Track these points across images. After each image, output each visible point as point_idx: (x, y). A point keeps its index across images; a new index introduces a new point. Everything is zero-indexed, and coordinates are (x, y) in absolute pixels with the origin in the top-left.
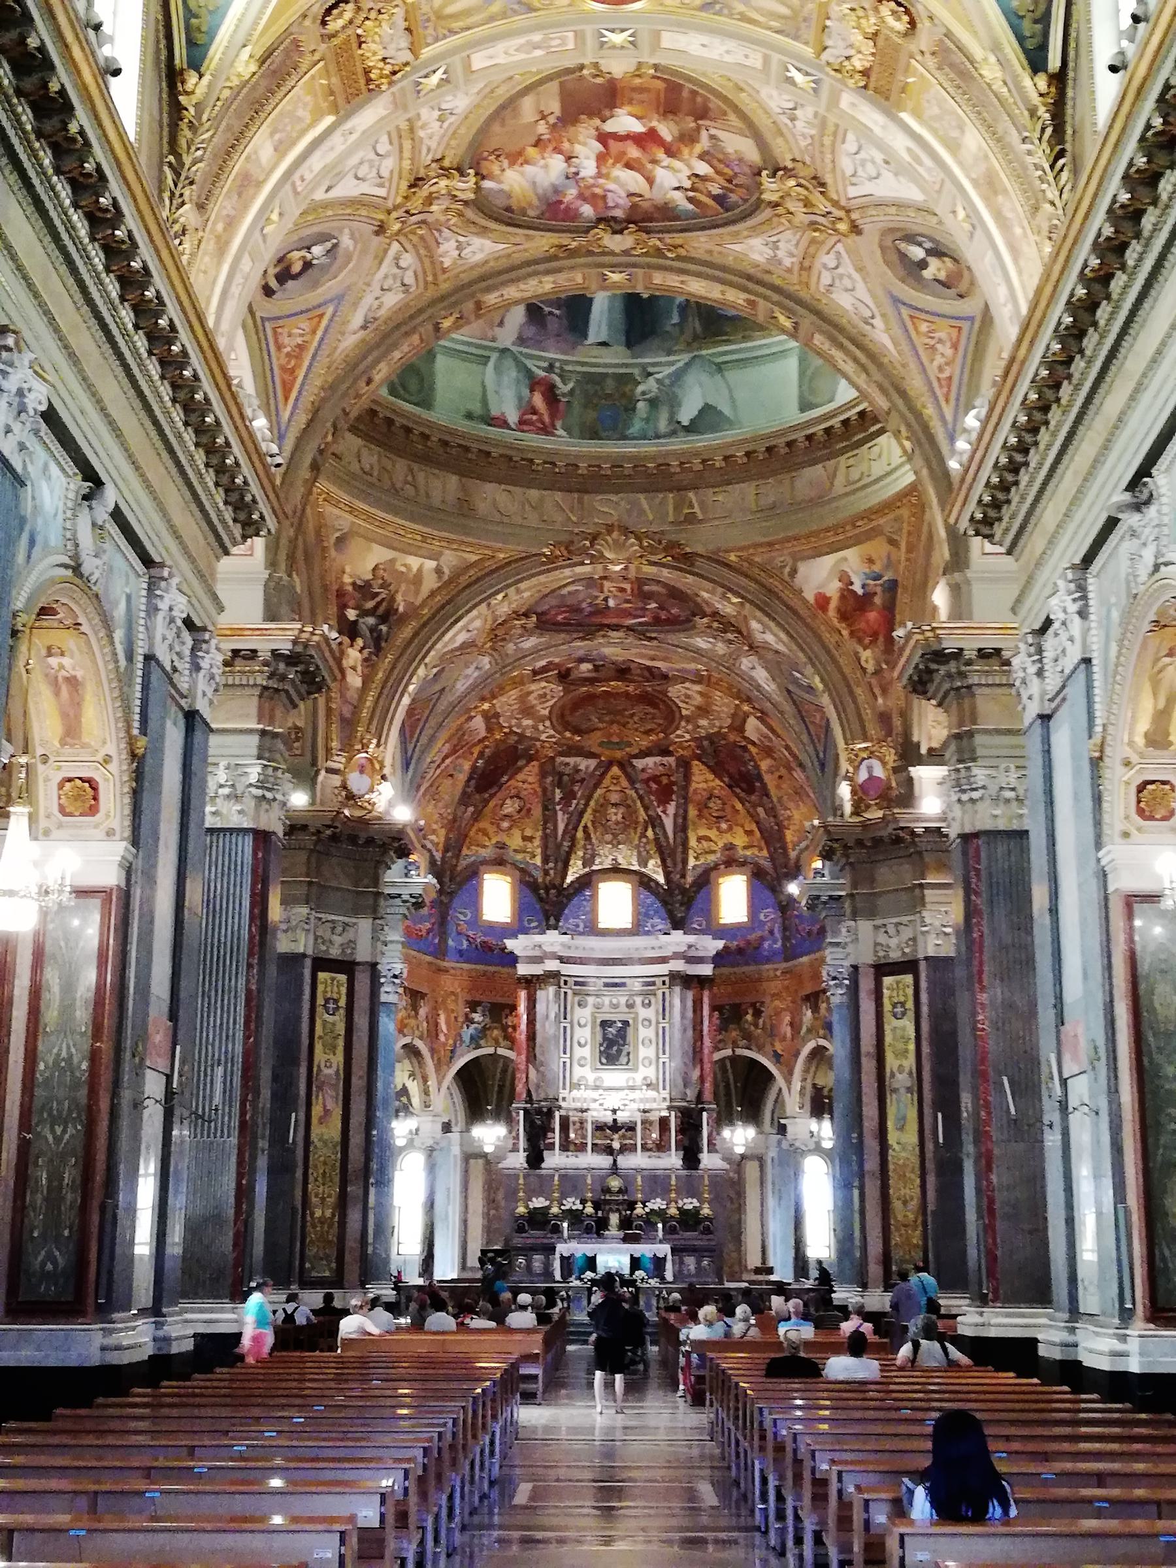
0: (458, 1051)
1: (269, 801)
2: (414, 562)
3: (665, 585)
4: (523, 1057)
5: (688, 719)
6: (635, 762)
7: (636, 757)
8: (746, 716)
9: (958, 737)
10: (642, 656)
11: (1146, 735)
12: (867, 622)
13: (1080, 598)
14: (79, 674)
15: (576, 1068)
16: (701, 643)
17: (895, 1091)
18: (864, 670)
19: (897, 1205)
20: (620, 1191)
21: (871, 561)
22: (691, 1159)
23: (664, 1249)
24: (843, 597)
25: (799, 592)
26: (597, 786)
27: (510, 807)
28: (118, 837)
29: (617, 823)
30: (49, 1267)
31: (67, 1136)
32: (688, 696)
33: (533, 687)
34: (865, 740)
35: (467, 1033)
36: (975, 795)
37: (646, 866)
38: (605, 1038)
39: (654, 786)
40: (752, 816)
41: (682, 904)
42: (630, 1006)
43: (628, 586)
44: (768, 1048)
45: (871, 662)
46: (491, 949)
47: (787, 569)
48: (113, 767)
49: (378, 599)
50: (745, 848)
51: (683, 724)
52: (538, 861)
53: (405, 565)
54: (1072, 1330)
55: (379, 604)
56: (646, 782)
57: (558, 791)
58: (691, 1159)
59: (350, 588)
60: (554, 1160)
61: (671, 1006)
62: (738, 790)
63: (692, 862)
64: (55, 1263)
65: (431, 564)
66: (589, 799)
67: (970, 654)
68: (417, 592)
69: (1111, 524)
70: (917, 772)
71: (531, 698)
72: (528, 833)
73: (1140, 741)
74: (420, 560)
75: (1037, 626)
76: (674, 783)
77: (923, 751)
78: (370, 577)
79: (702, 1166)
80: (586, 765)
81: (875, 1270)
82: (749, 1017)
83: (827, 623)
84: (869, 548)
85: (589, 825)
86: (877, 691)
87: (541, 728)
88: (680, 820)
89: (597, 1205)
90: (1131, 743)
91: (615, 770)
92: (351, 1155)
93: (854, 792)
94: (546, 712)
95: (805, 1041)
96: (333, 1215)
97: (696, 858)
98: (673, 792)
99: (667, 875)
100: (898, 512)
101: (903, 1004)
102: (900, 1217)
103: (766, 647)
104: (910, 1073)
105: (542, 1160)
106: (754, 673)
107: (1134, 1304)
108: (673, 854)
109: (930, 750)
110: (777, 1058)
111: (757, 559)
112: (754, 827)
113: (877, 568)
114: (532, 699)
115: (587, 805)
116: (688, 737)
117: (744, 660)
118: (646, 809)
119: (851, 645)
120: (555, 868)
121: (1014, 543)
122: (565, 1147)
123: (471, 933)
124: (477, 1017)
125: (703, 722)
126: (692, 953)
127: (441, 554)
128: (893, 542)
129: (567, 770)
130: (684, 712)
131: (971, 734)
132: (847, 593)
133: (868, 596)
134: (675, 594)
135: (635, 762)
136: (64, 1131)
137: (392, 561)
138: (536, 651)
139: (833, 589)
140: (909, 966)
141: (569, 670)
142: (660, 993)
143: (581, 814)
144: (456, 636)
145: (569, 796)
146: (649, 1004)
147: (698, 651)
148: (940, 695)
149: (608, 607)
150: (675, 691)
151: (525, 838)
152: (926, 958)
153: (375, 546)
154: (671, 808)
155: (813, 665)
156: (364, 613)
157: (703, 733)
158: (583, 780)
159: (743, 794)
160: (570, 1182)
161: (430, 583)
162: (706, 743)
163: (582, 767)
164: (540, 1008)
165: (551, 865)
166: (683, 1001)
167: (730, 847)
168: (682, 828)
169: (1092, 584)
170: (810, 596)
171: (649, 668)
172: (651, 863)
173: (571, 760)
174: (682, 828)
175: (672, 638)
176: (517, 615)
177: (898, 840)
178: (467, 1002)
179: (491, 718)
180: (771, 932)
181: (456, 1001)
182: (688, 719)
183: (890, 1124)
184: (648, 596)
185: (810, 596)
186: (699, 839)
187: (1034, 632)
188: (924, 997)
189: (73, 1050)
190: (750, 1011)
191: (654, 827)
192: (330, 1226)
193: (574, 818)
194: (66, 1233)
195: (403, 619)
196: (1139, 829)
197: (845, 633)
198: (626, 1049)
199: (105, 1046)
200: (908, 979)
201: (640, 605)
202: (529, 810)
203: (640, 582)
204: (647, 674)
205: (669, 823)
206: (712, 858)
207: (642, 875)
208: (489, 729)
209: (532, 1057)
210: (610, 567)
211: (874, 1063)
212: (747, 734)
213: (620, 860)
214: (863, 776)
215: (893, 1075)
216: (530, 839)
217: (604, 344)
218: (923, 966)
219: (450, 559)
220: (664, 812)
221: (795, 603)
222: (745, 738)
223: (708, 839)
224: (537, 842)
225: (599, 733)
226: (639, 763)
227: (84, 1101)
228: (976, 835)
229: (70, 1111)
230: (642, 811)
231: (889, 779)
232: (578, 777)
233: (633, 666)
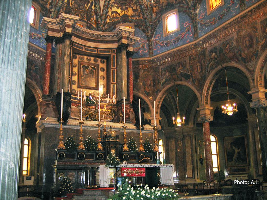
37: (89, 21)
50: (131, 16)
63: (108, 21)
97: (110, 20)
108: (102, 15)
112: (138, 7)
165: (53, 10)
172: (92, 19)
180: (143, 47)
191: (95, 5)
223: (116, 12)
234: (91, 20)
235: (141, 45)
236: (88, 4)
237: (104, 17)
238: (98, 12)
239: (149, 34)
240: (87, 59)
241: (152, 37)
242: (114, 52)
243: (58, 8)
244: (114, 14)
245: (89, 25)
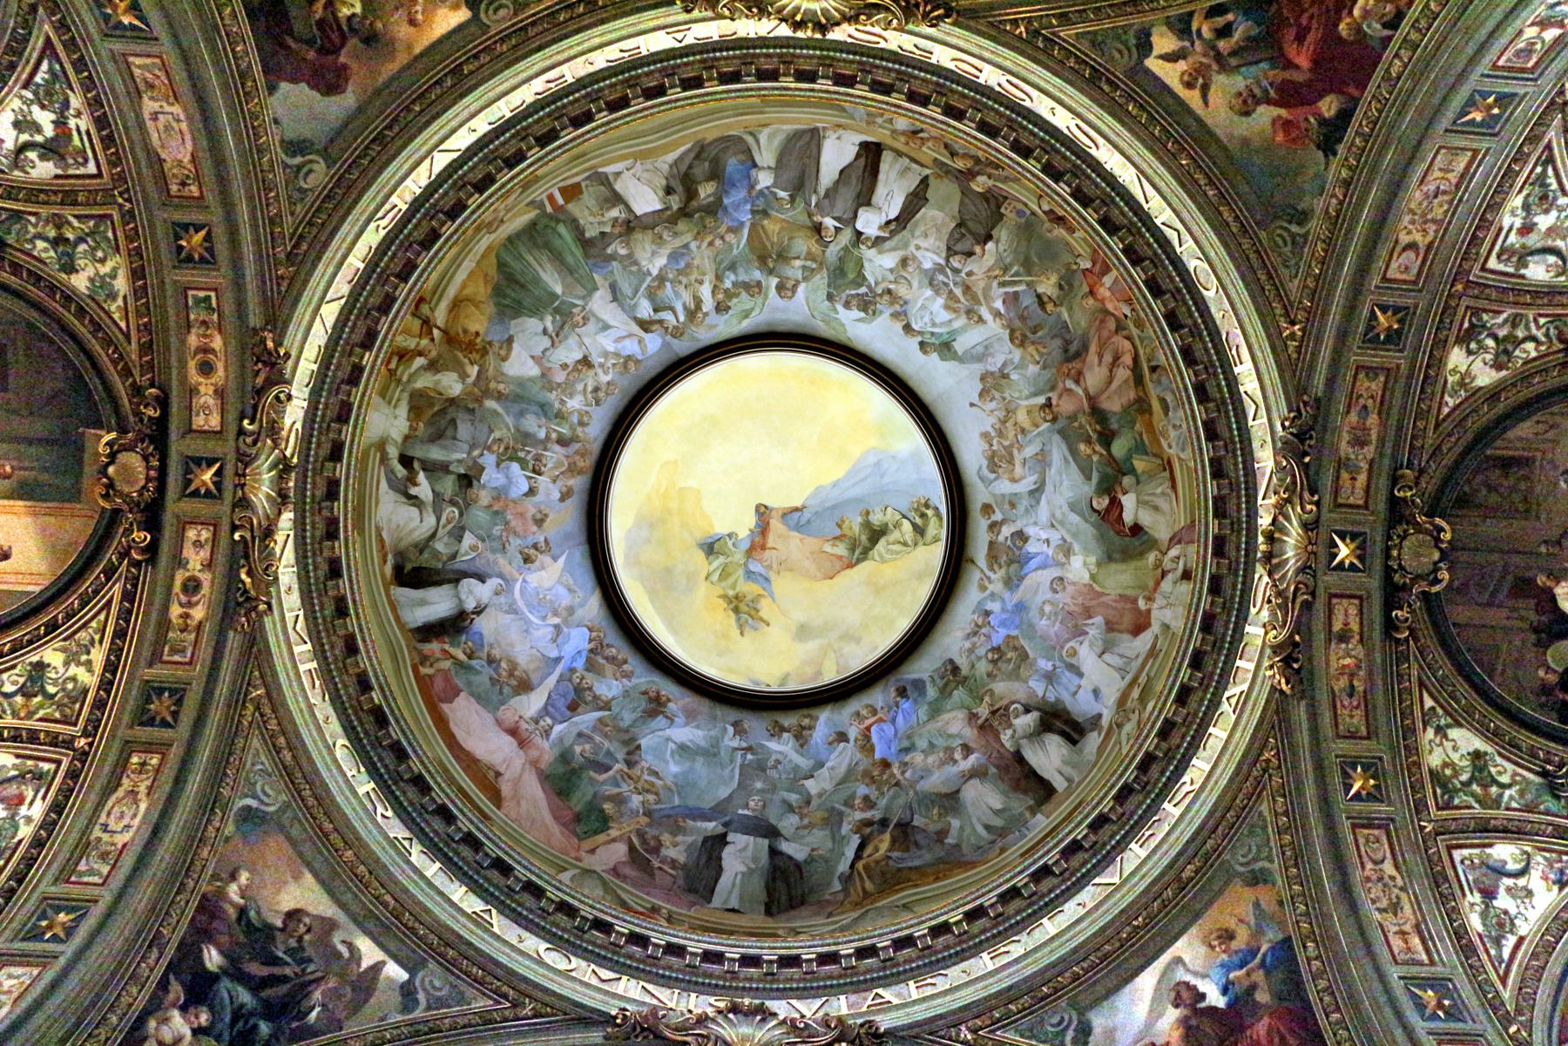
2: (369, 952)
53: (350, 946)
59: (232, 913)
65: (395, 972)
68: (356, 1007)
74: (378, 955)
78: (279, 923)
113: (1241, 941)
128: (1257, 879)
133: (1241, 1005)
137: (330, 925)
153: (309, 878)
161: (384, 1003)
217: (733, 910)
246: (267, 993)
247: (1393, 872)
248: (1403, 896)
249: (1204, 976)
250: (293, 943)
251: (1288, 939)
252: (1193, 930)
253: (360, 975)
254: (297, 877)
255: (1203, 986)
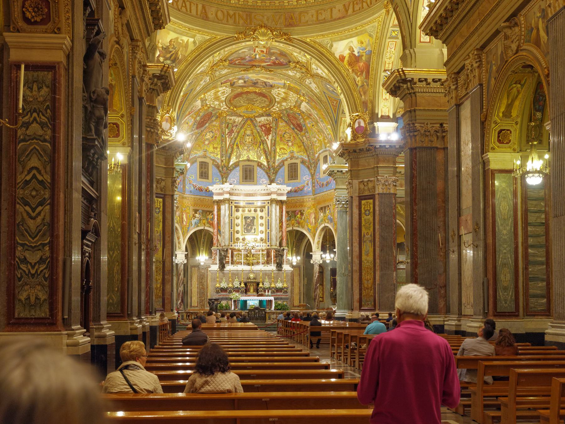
0: (191, 228)
1: (152, 133)
2: (185, 39)
3: (279, 50)
4: (216, 230)
5: (278, 103)
6: (256, 119)
7: (257, 117)
8: (302, 101)
9: (410, 111)
10: (262, 77)
11: (503, 113)
12: (359, 67)
13: (479, 61)
14: (113, 83)
15: (236, 234)
16: (290, 73)
17: (365, 242)
18: (357, 85)
19: (365, 282)
20: (254, 278)
21: (362, 43)
22: (279, 265)
23: (272, 298)
24: (350, 57)
25: (333, 54)
26: (241, 128)
27: (209, 136)
28: (127, 145)
29: (249, 142)
30: (111, 301)
31: (114, 255)
32: (279, 94)
33: (220, 89)
34: (358, 112)
35: (193, 221)
36: (416, 133)
38: (246, 223)
39: (264, 128)
40: (301, 141)
41: (273, 173)
42: (255, 211)
43: (265, 50)
44: (306, 226)
45: (360, 82)
46: (202, 190)
47: (329, 45)
48: (125, 119)
49: (172, 53)
51: (276, 104)
52: (219, 156)
53: (182, 40)
54: (459, 321)
55: (172, 55)
56: (261, 127)
57: (227, 130)
58: (279, 265)
60: (229, 268)
61: (271, 211)
62: (296, 130)
63: (277, 157)
64: (113, 300)
65: (191, 40)
66: (239, 133)
67: (416, 80)
68: (186, 51)
69: (497, 32)
70: (378, 125)
71: (219, 93)
72: (215, 146)
73: (501, 115)
75: (456, 71)
76: (272, 127)
77: (379, 116)
79: (283, 269)
80: (238, 120)
81: (356, 304)
82: (299, 216)
83: (343, 67)
84: (361, 37)
85: (239, 143)
86: (362, 93)
87: (222, 105)
88: (273, 142)
89: (245, 284)
90: (498, 116)
91: (249, 122)
92: (166, 265)
93: (353, 132)
94: (224, 99)
95: (321, 224)
96: (160, 287)
98: (271, 131)
99: (268, 162)
100: (374, 24)
101: (369, 210)
102: (366, 286)
103: (318, 75)
104: (371, 235)
105: (225, 268)
106: (310, 86)
107: (488, 310)
108: (270, 153)
109: (382, 116)
110: (309, 230)
111: (317, 41)
114: (219, 94)
115: (237, 136)
116: (277, 109)
117: (307, 80)
118: (260, 137)
119: (354, 75)
120: (225, 159)
121: (446, 40)
122: (232, 263)
123: (194, 184)
124: (197, 215)
125: (284, 104)
126: (279, 192)
127: (195, 36)
129: (231, 122)
130: (277, 100)
131: (415, 111)
132: (352, 55)
134: (283, 54)
135: (256, 119)
136: (113, 253)
137: (177, 38)
138: (226, 75)
139: (346, 53)
140: (372, 197)
141: (234, 82)
142: (266, 207)
143: (236, 139)
144: (200, 69)
145: (231, 132)
146: (263, 211)
147: (289, 76)
148: (403, 95)
149: (256, 58)
150: (274, 92)
151: (214, 148)
152: (378, 194)
153: (171, 32)
154: (270, 137)
155: (338, 83)
156: (166, 59)
157: (283, 108)
158: (237, 126)
159: (298, 132)
160: (235, 274)
161: (191, 47)
162: (285, 112)
163: (237, 121)
164: (222, 212)
165: (224, 158)
166: (276, 210)
167: (292, 152)
168: (274, 144)
169: (484, 57)
170: (337, 56)
171: (265, 83)
172: (262, 157)
173: (233, 118)
174: (274, 144)
175: (279, 71)
176: (221, 60)
177: (368, 150)
178: (193, 210)
179: (203, 100)
180: (308, 184)
181: (189, 209)
182: (278, 103)
183: (363, 254)
184: (273, 54)
185: (337, 56)
186: (280, 149)
187: (455, 73)
188: (377, 208)
189: (115, 224)
190: (299, 214)
191: (263, 144)
192: (160, 291)
193: (233, 141)
194: (116, 289)
195: (180, 62)
196: (498, 147)
197: (350, 70)
198: (254, 228)
199: (126, 223)
200: (371, 201)
201: (269, 57)
202: (216, 137)
203: (269, 49)
204: (264, 84)
205: (269, 143)
206: (285, 156)
207: (259, 162)
208: (202, 106)
209: (219, 231)
210: (260, 42)
211: (358, 232)
212: (301, 109)
213: (250, 156)
214: (356, 125)
215: (364, 236)
216: (216, 148)
218: (377, 196)
219: (199, 37)
220: (267, 138)
221: (331, 58)
222: (300, 110)
223: (284, 149)
224: (218, 150)
225: (243, 108)
226: (258, 119)
227: (120, 243)
228: (415, 149)
229: (115, 246)
230: (258, 137)
231: (366, 127)
232: (235, 124)
233: (259, 81)
234: (261, 159)
235: (306, 182)
236: (256, 145)
237: (272, 155)
238: (267, 150)
239: (313, 171)
240: (248, 210)
241: (314, 174)
242: (268, 203)
243: (229, 155)
244: (282, 150)
245: (260, 164)
246: (171, 59)
247: (394, 51)
248: (393, 55)
249: (356, 48)
250: (172, 46)
251: (371, 51)
252: (356, 37)
253: (185, 44)
254: (169, 34)
255: (355, 49)
